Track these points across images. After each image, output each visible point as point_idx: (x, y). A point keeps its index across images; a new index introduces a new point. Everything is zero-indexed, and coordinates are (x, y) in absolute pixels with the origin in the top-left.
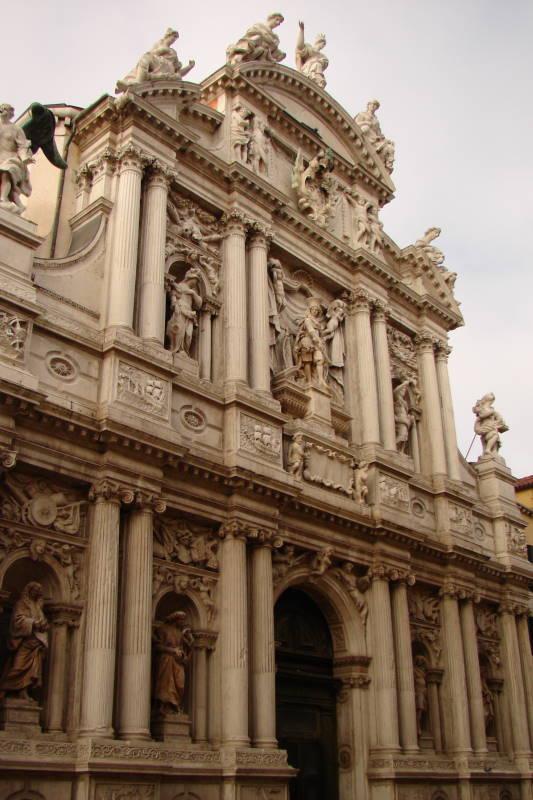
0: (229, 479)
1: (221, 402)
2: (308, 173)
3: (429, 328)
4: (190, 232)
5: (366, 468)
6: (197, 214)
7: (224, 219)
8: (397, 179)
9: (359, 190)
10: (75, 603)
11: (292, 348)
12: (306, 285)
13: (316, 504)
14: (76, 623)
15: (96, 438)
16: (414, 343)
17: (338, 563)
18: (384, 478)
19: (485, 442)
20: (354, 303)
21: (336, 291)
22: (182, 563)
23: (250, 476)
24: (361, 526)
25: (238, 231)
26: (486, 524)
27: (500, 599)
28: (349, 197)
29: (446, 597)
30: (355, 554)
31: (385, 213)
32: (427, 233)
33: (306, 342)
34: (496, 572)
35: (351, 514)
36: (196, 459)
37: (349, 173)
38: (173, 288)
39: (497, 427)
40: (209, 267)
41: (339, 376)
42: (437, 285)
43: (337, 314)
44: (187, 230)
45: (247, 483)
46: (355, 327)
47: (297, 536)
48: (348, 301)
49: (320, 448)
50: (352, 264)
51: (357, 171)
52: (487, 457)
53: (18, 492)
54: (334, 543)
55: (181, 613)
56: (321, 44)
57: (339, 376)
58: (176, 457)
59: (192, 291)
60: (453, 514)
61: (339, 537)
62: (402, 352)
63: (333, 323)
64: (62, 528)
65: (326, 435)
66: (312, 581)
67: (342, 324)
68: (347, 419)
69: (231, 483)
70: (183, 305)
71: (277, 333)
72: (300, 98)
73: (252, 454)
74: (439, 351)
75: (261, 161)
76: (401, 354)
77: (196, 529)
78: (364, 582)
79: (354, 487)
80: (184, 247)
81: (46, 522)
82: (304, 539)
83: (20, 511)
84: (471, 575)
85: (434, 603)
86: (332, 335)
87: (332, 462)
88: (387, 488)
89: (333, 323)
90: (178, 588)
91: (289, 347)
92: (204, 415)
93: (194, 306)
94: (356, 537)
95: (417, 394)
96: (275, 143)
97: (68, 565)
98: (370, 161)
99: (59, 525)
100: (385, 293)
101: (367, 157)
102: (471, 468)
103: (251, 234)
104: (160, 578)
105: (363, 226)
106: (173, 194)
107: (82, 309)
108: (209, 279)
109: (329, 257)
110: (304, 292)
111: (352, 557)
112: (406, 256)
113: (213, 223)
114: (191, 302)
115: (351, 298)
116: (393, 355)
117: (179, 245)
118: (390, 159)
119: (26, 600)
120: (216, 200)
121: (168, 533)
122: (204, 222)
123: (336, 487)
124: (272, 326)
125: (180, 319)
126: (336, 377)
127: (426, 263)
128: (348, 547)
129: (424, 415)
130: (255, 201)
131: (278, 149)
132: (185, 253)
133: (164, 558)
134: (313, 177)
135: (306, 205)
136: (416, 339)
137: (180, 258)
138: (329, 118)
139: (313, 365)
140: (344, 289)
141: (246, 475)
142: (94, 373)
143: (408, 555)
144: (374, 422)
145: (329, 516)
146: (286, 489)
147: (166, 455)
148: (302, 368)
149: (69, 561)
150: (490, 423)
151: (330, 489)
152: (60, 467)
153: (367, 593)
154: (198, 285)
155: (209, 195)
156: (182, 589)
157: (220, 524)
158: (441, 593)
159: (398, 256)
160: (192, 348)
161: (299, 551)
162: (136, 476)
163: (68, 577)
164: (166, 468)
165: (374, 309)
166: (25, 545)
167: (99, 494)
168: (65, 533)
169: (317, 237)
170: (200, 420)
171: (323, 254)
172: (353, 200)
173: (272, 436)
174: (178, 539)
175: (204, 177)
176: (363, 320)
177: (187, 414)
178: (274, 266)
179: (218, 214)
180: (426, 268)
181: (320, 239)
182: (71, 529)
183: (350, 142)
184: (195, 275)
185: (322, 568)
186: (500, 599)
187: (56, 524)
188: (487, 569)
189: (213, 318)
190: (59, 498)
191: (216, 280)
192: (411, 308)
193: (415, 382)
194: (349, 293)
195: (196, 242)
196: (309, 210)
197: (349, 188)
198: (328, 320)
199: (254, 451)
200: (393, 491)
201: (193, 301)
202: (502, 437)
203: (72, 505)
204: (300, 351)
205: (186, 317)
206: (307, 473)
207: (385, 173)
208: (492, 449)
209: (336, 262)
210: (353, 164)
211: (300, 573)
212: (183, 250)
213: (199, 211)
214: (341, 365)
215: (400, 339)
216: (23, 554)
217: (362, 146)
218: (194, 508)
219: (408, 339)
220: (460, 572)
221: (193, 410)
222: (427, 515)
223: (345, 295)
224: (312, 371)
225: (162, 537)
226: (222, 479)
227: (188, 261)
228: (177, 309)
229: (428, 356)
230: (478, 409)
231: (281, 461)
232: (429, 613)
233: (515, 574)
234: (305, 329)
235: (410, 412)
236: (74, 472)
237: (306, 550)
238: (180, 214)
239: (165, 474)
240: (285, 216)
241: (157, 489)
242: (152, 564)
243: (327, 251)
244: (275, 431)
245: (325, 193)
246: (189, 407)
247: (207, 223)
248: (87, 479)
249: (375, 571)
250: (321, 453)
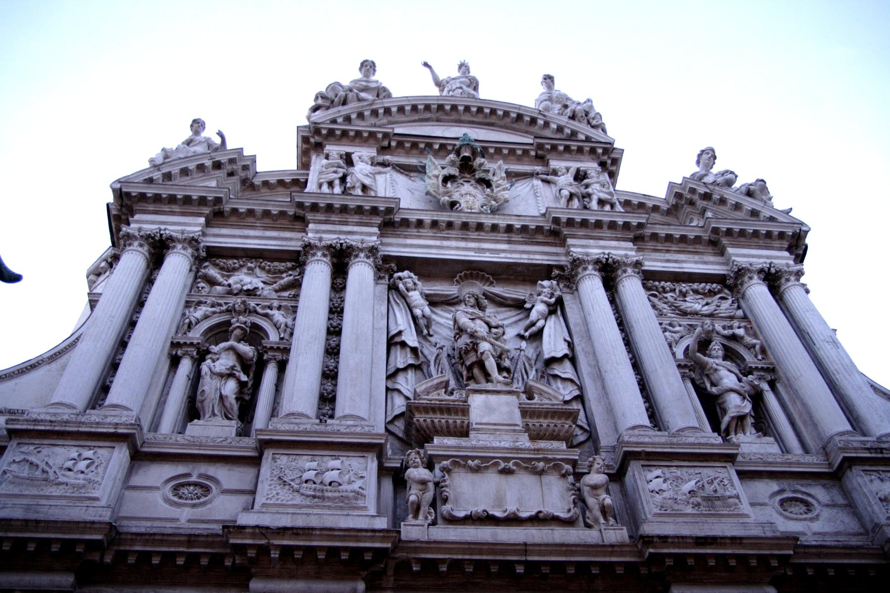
8: (617, 133)
23: (264, 535)
32: (698, 163)
37: (533, 153)
45: (264, 550)
51: (540, 147)
56: (463, 68)
72: (438, 120)
87: (511, 479)
95: (754, 346)
112: (673, 201)
118: (592, 115)
120: (284, 243)
138: (488, 121)
141: (253, 536)
146: (357, 539)
159: (665, 207)
172: (549, 177)
175: (266, 228)
192: (700, 248)
193: (741, 332)
210: (531, 141)
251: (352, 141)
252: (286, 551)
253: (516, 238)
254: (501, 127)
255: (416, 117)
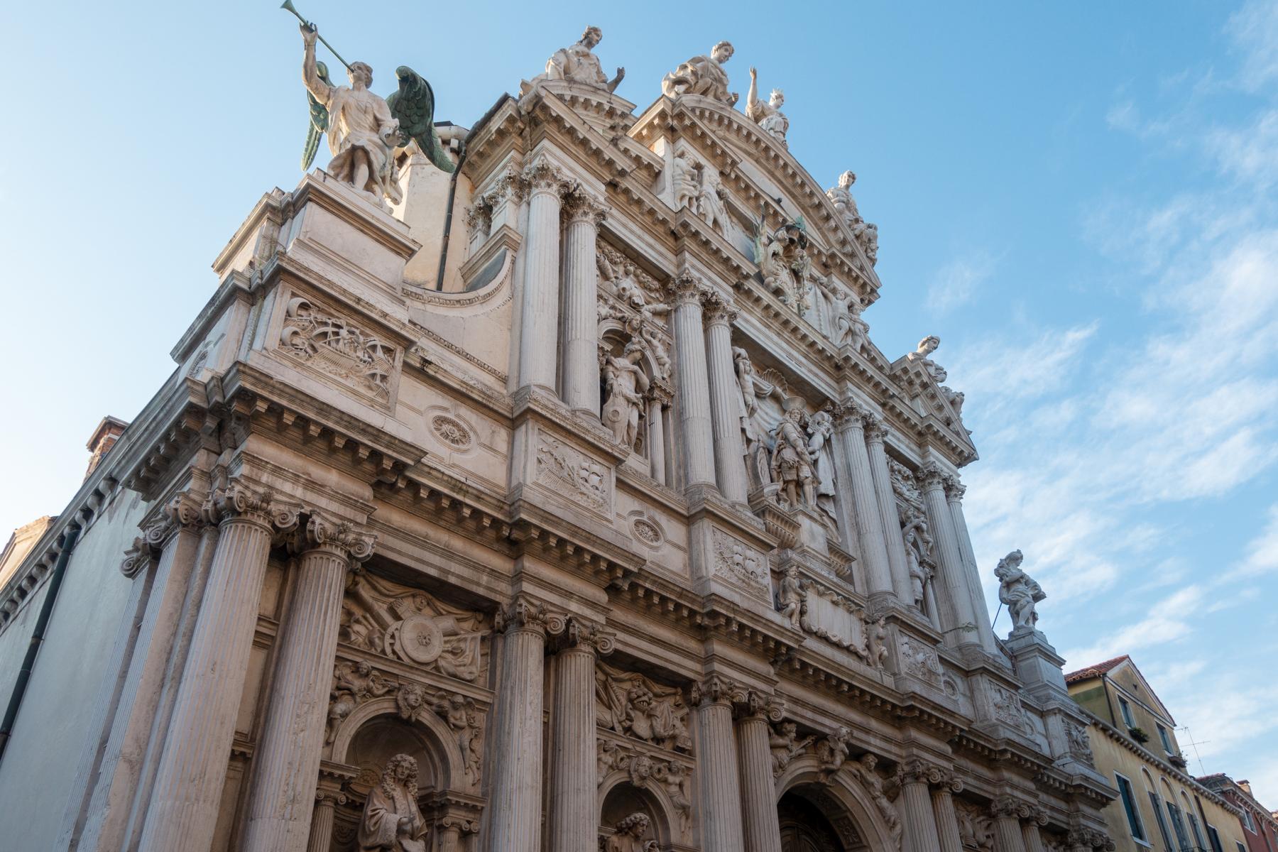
0: (702, 615)
1: (685, 513)
2: (777, 247)
3: (938, 459)
4: (628, 293)
5: (882, 622)
6: (636, 276)
7: (670, 286)
9: (837, 282)
10: (471, 791)
11: (769, 465)
12: (779, 390)
13: (827, 665)
14: (474, 827)
15: (506, 532)
16: (917, 479)
17: (857, 755)
18: (906, 639)
19: (1015, 614)
20: (841, 417)
21: (817, 401)
22: (640, 738)
24: (884, 702)
25: (691, 300)
26: (1035, 719)
27: (1068, 824)
28: (826, 291)
29: (1002, 815)
30: (878, 742)
31: (866, 315)
33: (788, 454)
34: (1061, 783)
35: (872, 683)
36: (657, 580)
38: (608, 362)
39: (1030, 593)
40: (655, 342)
41: (829, 507)
42: (940, 408)
43: (823, 429)
44: (624, 289)
45: (729, 621)
46: (845, 447)
47: (799, 710)
48: (835, 416)
49: (822, 588)
50: (838, 368)
52: (1022, 632)
53: (381, 609)
54: (850, 723)
55: (640, 815)
57: (829, 507)
58: (627, 573)
59: (636, 368)
60: (998, 698)
61: (855, 717)
62: (904, 488)
63: (818, 440)
64: (452, 670)
65: (825, 573)
66: (822, 779)
67: (828, 441)
68: (848, 559)
69: (707, 622)
70: (624, 385)
71: (749, 441)
73: (732, 584)
74: (952, 489)
75: (715, 222)
76: (905, 490)
77: (658, 689)
78: (894, 785)
79: (868, 647)
80: (621, 311)
81: (423, 656)
82: (809, 714)
83: (382, 638)
84: (1031, 786)
85: (985, 824)
86: (817, 454)
88: (910, 652)
89: (818, 440)
90: (634, 775)
91: (764, 461)
92: (661, 529)
93: (639, 387)
94: (876, 718)
95: (928, 542)
96: (731, 209)
97: (462, 728)
98: (848, 249)
99: (448, 663)
100: (880, 409)
101: (844, 243)
102: (1001, 645)
103: (710, 307)
104: (609, 759)
105: (845, 324)
106: (603, 244)
107: (482, 366)
108: (657, 359)
109: (806, 357)
110: (775, 397)
111: (875, 746)
113: (657, 290)
114: (634, 383)
115: (836, 411)
116: (895, 490)
117: (613, 307)
119: (390, 784)
120: (660, 259)
121: (620, 693)
122: (645, 287)
123: (845, 644)
124: (743, 430)
125: (621, 400)
126: (826, 508)
127: (925, 379)
128: (867, 731)
129: (939, 568)
130: (710, 267)
131: (734, 219)
132: (622, 320)
133: (612, 728)
134: (781, 252)
135: (773, 285)
136: (919, 475)
137: (616, 326)
139: (799, 484)
140: (828, 398)
142: (502, 446)
143: (948, 749)
144: (888, 567)
145: (840, 682)
146: (782, 634)
147: (612, 566)
148: (783, 490)
149: (464, 723)
150: (1021, 587)
151: (838, 646)
152: (448, 572)
153: (901, 801)
154: (642, 362)
155: (653, 253)
156: (643, 778)
157: (690, 682)
158: (994, 810)
160: (640, 443)
161: (803, 733)
162: (568, 594)
163: (462, 749)
164: (612, 590)
165: (869, 427)
166: (389, 692)
167: (512, 619)
168: (455, 676)
169: (792, 326)
170: (656, 534)
171: (799, 351)
172: (830, 295)
173: (760, 564)
174: (631, 701)
176: (856, 435)
177: (638, 523)
178: (739, 355)
179: (664, 279)
180: (925, 386)
181: (795, 330)
182: (464, 673)
183: (821, 224)
184: (638, 347)
185: (839, 759)
186: (1068, 824)
187: (442, 663)
188: (1049, 777)
189: (665, 408)
190: (448, 623)
191: (666, 359)
192: (911, 434)
193: (924, 526)
194: (833, 404)
195: (635, 307)
196: (778, 292)
197: (825, 280)
198: (810, 436)
199: (734, 580)
200: (920, 657)
201: (638, 382)
202: (1038, 607)
203: (469, 636)
204: (780, 467)
205: (628, 400)
206: (805, 618)
207: (867, 264)
208: (1027, 622)
209: (815, 364)
211: (807, 765)
212: (619, 315)
213: (639, 271)
214: (831, 492)
215: (899, 472)
216: (386, 707)
217: (836, 229)
218: (655, 656)
219: (909, 472)
220: (1016, 779)
221: (645, 519)
222: (961, 700)
223: (829, 407)
224: (798, 494)
225: (607, 693)
226: (692, 613)
227: (628, 330)
228: (616, 389)
229: (938, 493)
230: (1001, 571)
231: (771, 598)
232: (983, 839)
233: (1086, 788)
234: (786, 438)
235: (921, 564)
236: (472, 582)
237: (811, 732)
238: (614, 271)
239: (609, 601)
240: (749, 293)
241: (601, 619)
242: (595, 736)
243: (803, 347)
244: (761, 558)
245: (796, 274)
246: (640, 513)
247: (651, 290)
248: (492, 596)
249: (907, 769)
250: (820, 594)
251: (694, 140)
252: (742, 627)
253: (812, 356)
254: (799, 204)
255: (744, 146)
